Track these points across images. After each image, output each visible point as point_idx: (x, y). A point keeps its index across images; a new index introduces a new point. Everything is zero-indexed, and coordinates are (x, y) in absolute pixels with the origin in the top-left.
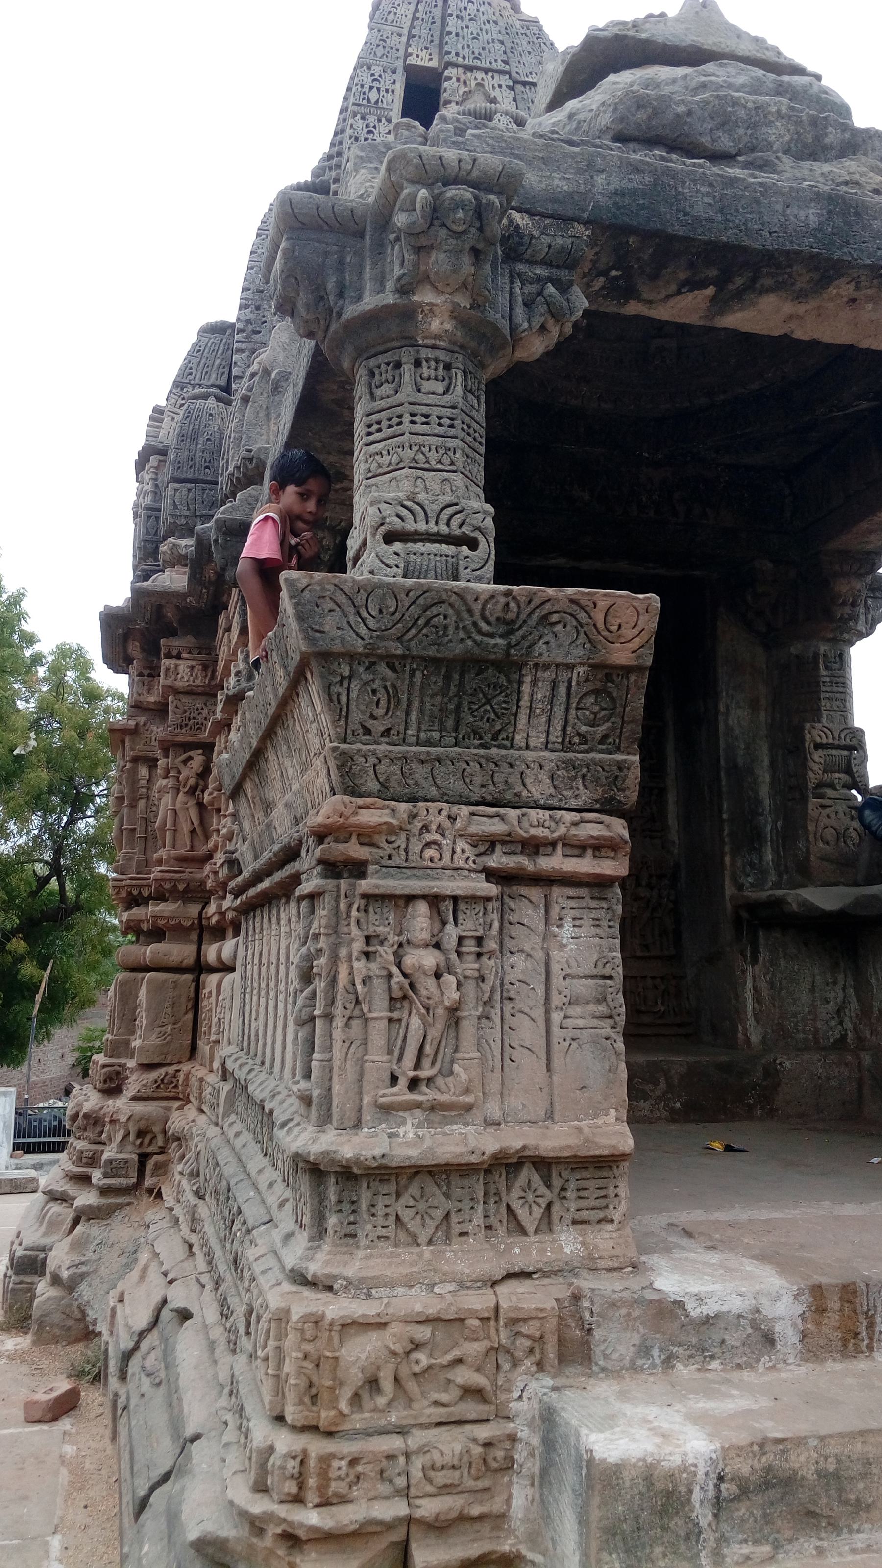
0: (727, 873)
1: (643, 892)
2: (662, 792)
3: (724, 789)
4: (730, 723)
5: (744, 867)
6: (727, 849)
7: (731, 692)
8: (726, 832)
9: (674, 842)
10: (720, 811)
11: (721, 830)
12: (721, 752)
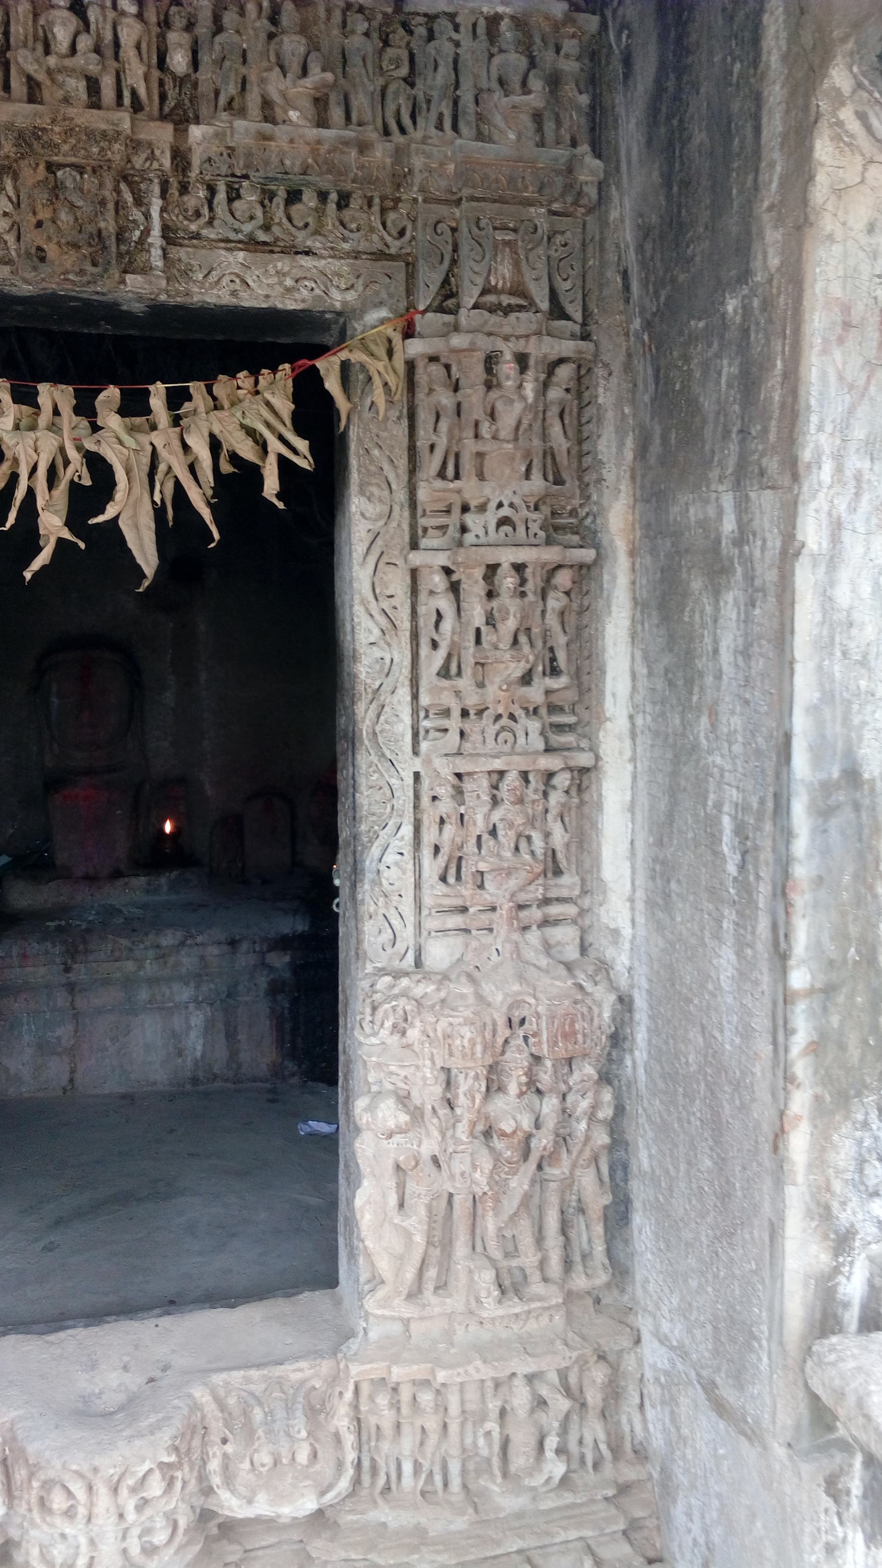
0: (796, 1197)
1: (510, 1112)
2: (584, 777)
3: (801, 872)
4: (842, 595)
5: (861, 1163)
6: (800, 1102)
7: (855, 462)
8: (800, 1039)
9: (616, 933)
10: (781, 957)
11: (781, 1029)
12: (800, 723)
